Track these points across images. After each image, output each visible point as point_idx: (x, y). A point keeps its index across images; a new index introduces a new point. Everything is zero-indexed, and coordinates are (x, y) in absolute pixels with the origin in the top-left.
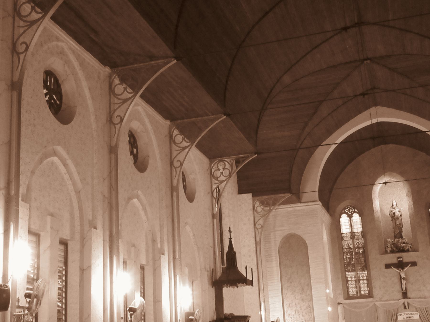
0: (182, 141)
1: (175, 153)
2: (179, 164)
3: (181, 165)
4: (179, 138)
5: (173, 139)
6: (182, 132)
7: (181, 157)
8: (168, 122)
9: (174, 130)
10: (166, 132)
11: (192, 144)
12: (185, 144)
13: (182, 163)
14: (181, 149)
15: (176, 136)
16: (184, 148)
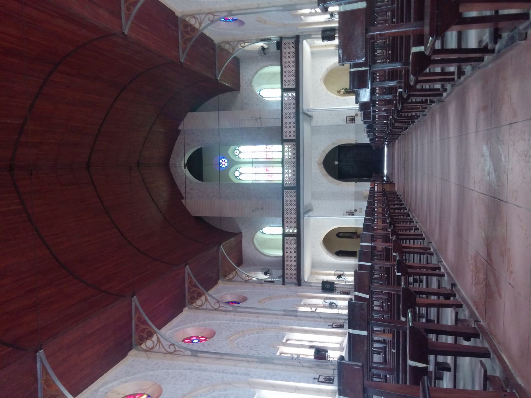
0: (152, 341)
1: (163, 350)
2: (172, 347)
3: (173, 345)
4: (149, 343)
5: (148, 349)
6: (142, 340)
7: (166, 344)
8: (132, 352)
9: (141, 348)
10: (143, 353)
11: (155, 332)
12: (154, 338)
13: (171, 344)
14: (158, 344)
15: (146, 346)
16: (159, 340)
